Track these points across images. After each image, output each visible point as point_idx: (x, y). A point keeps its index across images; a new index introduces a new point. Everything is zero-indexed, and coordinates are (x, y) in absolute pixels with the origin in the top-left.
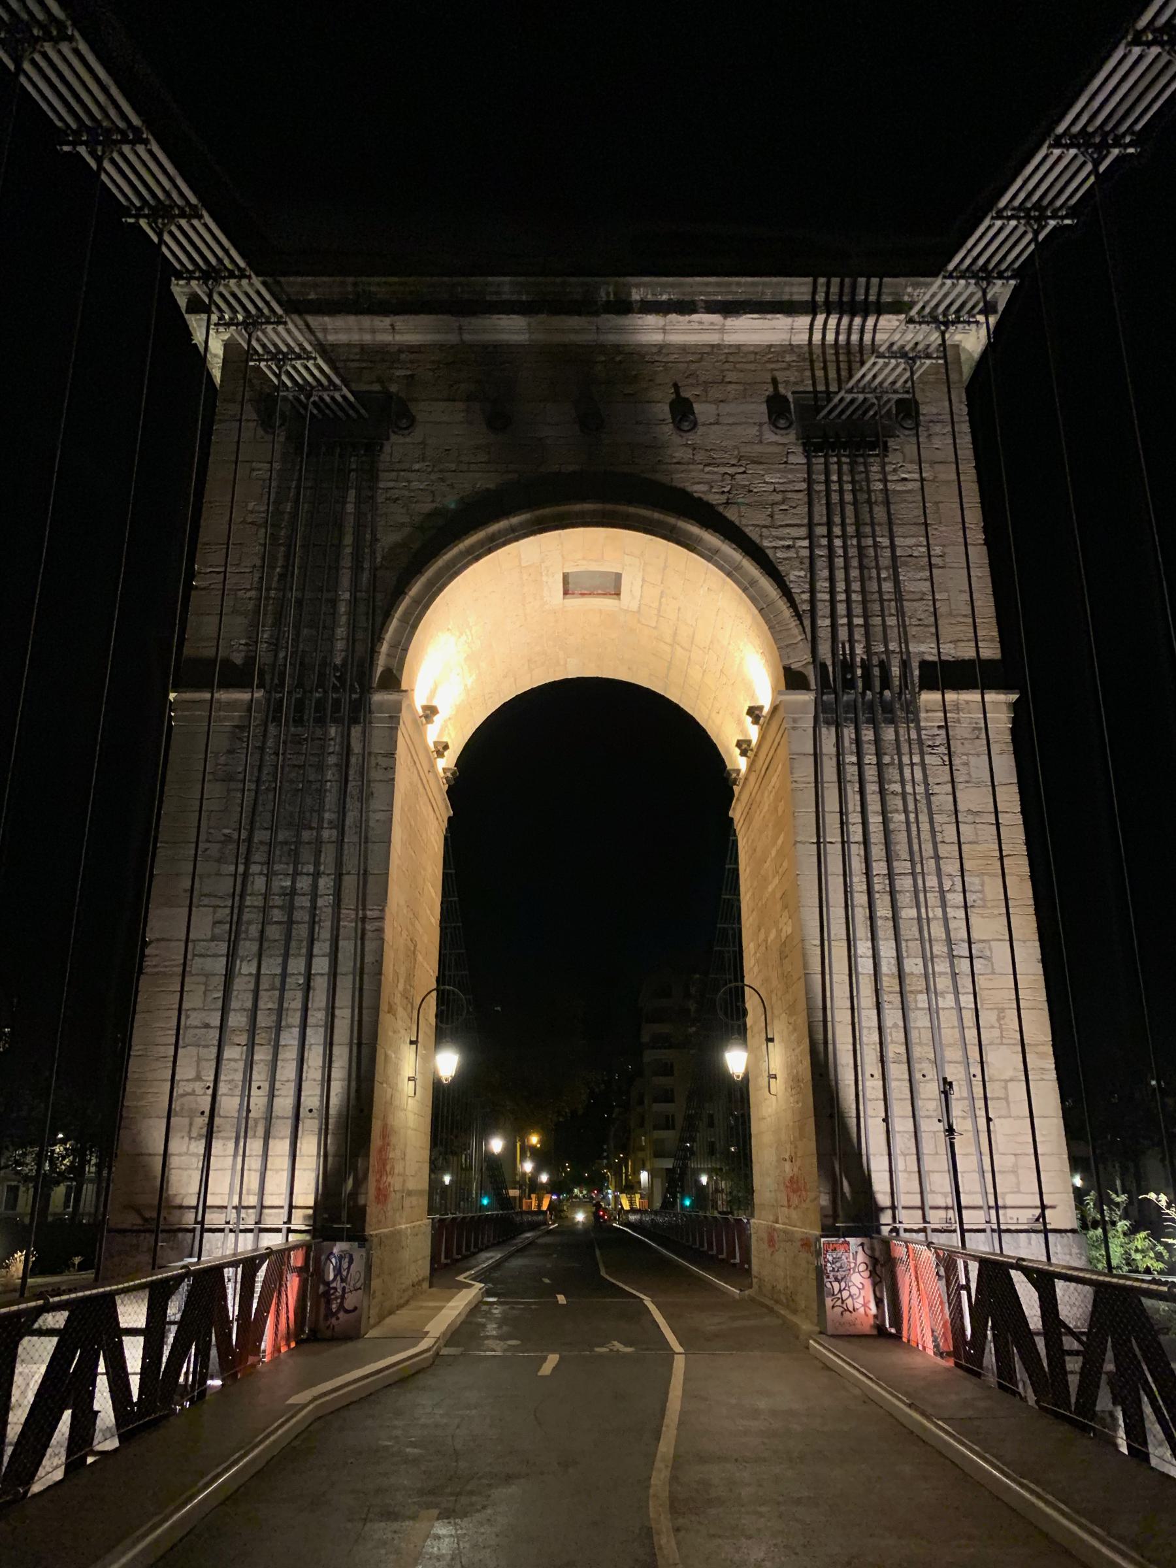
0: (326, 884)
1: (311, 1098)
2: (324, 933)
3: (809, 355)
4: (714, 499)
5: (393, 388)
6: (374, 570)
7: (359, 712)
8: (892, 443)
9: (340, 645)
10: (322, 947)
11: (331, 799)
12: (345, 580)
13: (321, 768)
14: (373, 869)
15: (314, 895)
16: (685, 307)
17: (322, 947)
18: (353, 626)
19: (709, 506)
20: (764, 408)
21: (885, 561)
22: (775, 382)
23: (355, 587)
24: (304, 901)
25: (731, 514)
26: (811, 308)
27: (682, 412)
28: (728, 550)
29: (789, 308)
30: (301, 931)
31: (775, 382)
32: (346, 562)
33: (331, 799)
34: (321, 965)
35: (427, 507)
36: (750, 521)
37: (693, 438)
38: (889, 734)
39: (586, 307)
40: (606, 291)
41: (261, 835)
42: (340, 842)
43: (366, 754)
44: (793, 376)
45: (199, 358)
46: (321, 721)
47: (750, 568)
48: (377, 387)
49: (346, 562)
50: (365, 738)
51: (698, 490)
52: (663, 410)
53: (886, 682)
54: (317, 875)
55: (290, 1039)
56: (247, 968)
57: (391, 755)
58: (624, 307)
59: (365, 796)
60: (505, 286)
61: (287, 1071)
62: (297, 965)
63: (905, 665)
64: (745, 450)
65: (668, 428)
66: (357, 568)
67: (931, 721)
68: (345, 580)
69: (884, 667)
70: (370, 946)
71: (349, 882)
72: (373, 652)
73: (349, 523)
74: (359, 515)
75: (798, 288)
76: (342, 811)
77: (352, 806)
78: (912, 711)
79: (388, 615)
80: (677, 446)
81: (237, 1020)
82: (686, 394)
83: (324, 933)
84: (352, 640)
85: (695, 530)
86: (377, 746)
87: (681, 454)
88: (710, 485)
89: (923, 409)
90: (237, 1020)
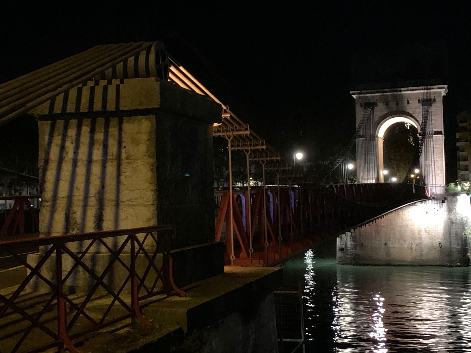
0: (373, 157)
1: (374, 177)
2: (373, 162)
3: (423, 94)
4: (412, 113)
5: (375, 101)
6: (375, 124)
7: (374, 140)
8: (432, 105)
9: (372, 132)
10: (373, 163)
11: (372, 149)
12: (372, 125)
13: (371, 146)
14: (377, 155)
15: (372, 158)
16: (408, 90)
17: (373, 163)
18: (373, 130)
19: (411, 114)
20: (417, 101)
21: (431, 119)
22: (419, 97)
23: (373, 126)
24: (371, 159)
25: (413, 115)
26: (423, 89)
27: (408, 102)
28: (413, 119)
29: (420, 90)
30: (371, 161)
31: (419, 97)
32: (372, 123)
33: (372, 149)
34: (373, 165)
35: (379, 116)
36: (415, 115)
37: (409, 105)
38: (430, 139)
39: (396, 91)
40: (399, 89)
41: (366, 153)
42: (374, 153)
43: (375, 144)
44: (421, 97)
45: (353, 98)
46: (371, 141)
47: (415, 121)
48: (373, 101)
49: (372, 123)
50: (375, 142)
51: (410, 112)
52: (406, 102)
53: (430, 134)
54: (372, 157)
55: (371, 171)
56: (366, 165)
57: (378, 144)
58: (401, 91)
59: (376, 149)
60: (387, 90)
61: (371, 174)
62: (371, 165)
63: (432, 132)
64: (415, 107)
65: (406, 104)
66: (373, 124)
67: (434, 138)
68: (372, 125)
69: (430, 132)
70: (378, 163)
71: (375, 157)
72: (375, 134)
73: (371, 118)
74: (373, 117)
75: (421, 88)
76: (373, 150)
77: (375, 150)
78: (432, 137)
79: (377, 129)
80: (407, 106)
81: (366, 170)
82: (408, 100)
83: (373, 162)
84: (373, 132)
85: (409, 117)
86: (376, 143)
87: (408, 108)
88: (411, 111)
89: (436, 100)
90: (366, 170)
